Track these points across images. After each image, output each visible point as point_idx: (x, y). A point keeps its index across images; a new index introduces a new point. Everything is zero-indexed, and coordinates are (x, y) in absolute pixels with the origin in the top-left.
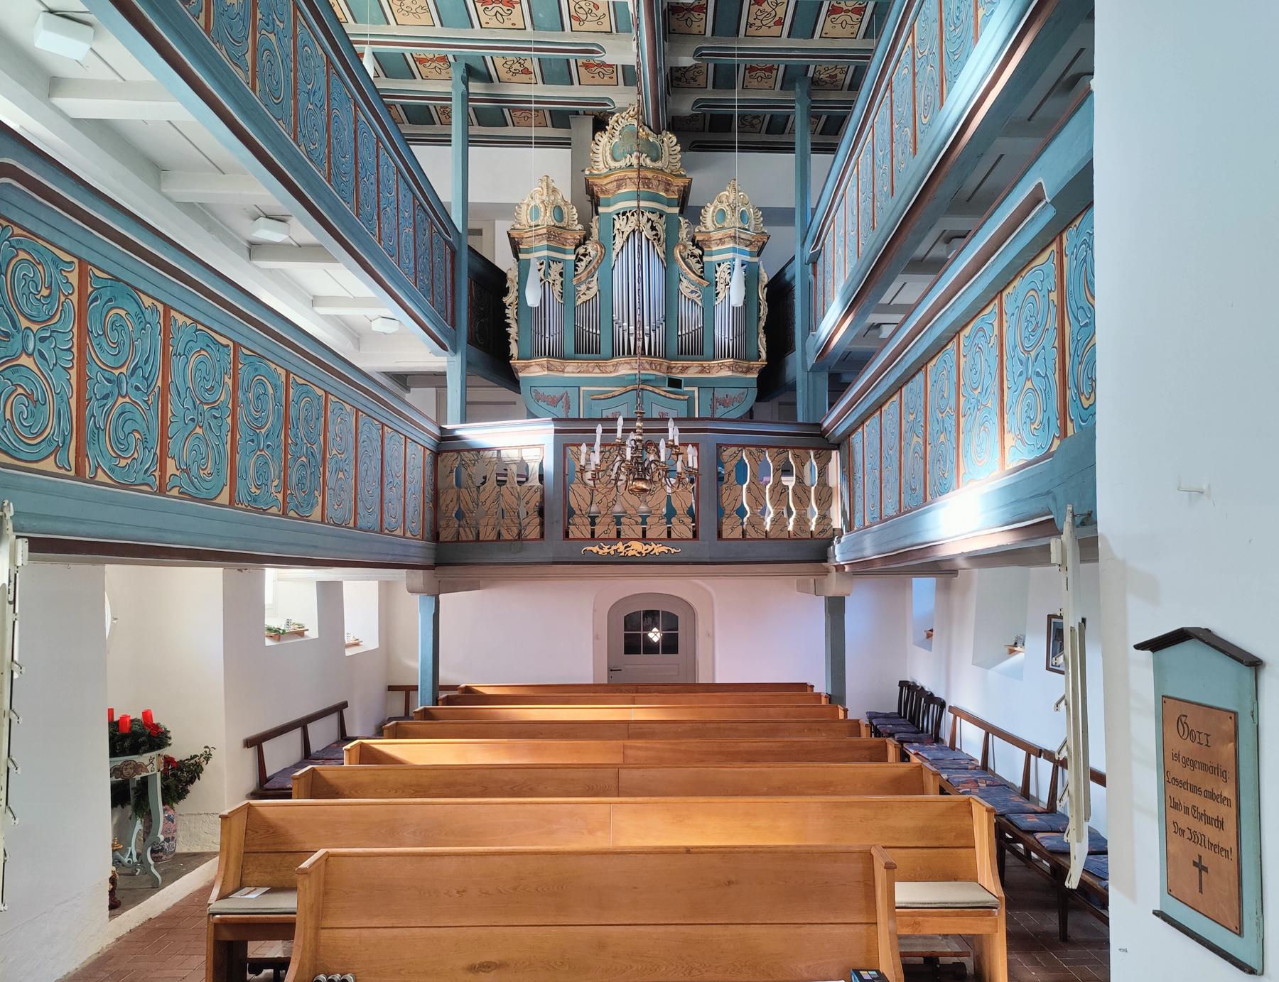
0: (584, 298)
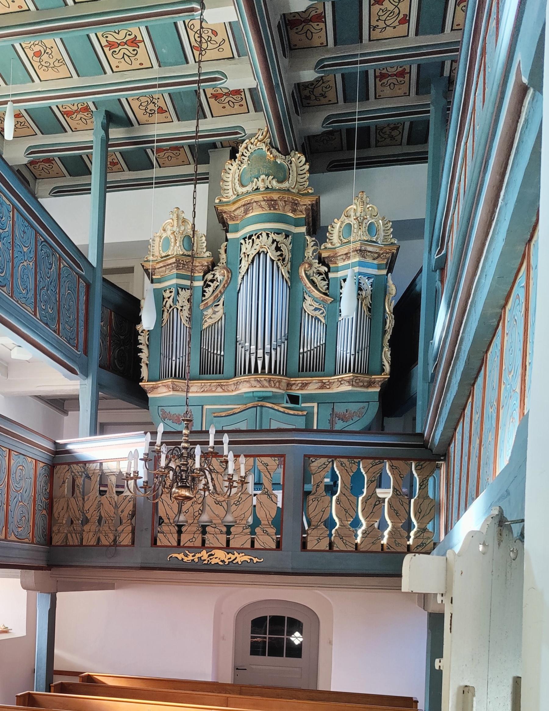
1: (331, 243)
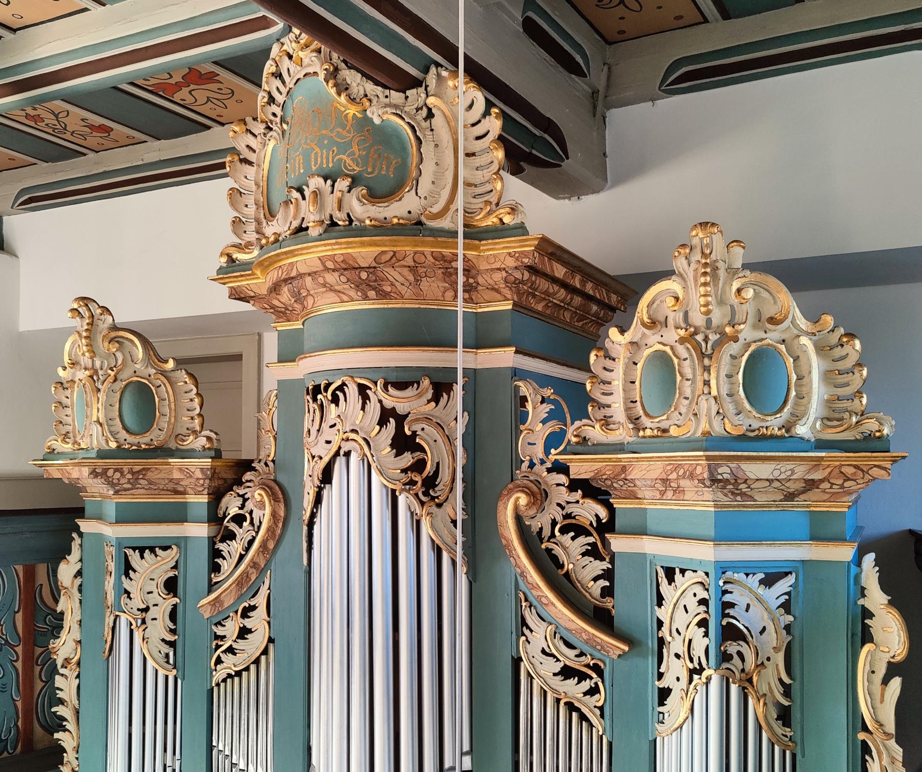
0: (231, 663)
1: (606, 422)
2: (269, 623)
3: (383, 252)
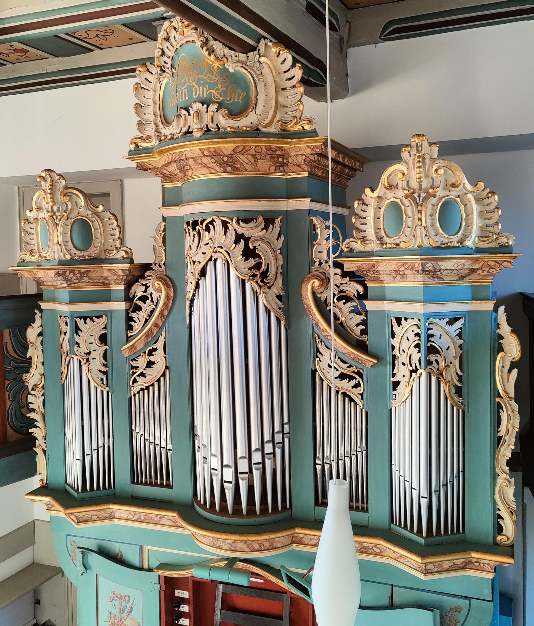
0: (142, 382)
1: (364, 240)
2: (165, 358)
3: (238, 146)
